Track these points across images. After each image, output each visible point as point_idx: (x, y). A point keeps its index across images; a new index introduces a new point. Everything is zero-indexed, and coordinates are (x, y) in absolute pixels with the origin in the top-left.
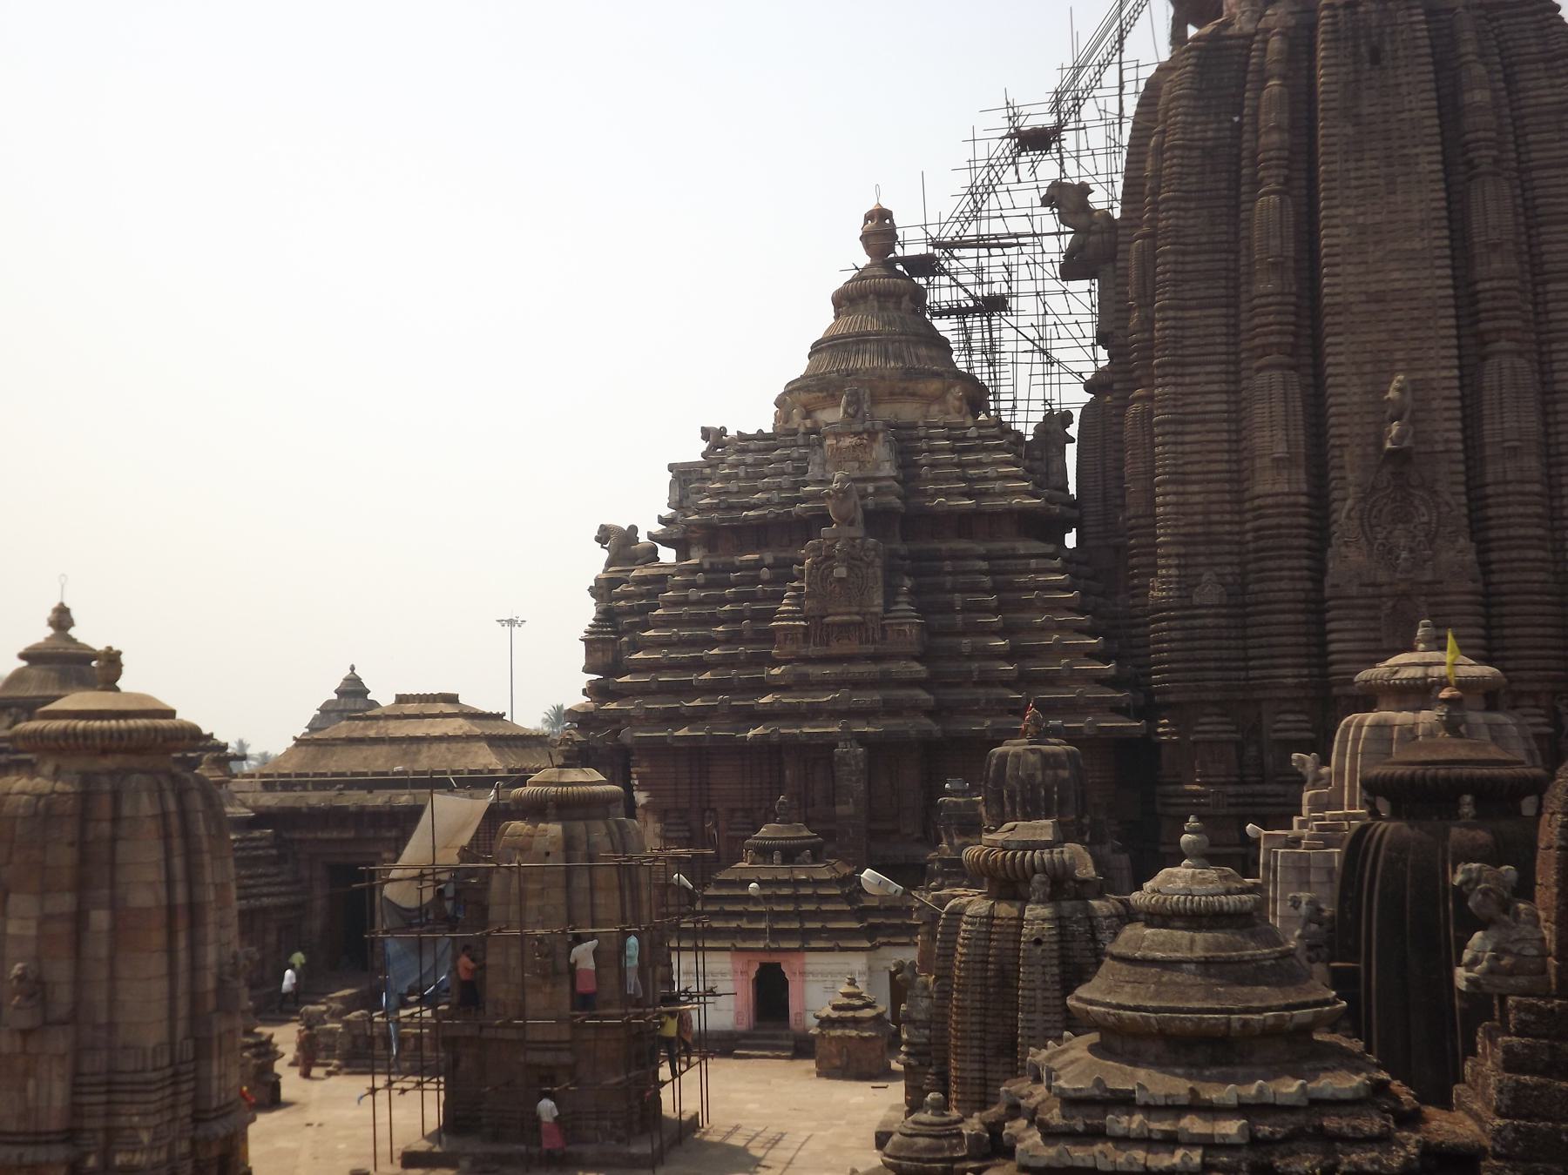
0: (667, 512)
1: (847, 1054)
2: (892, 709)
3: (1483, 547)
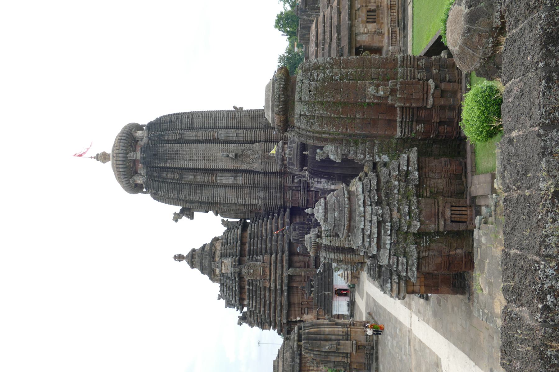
0: (236, 309)
1: (355, 278)
3: (256, 141)
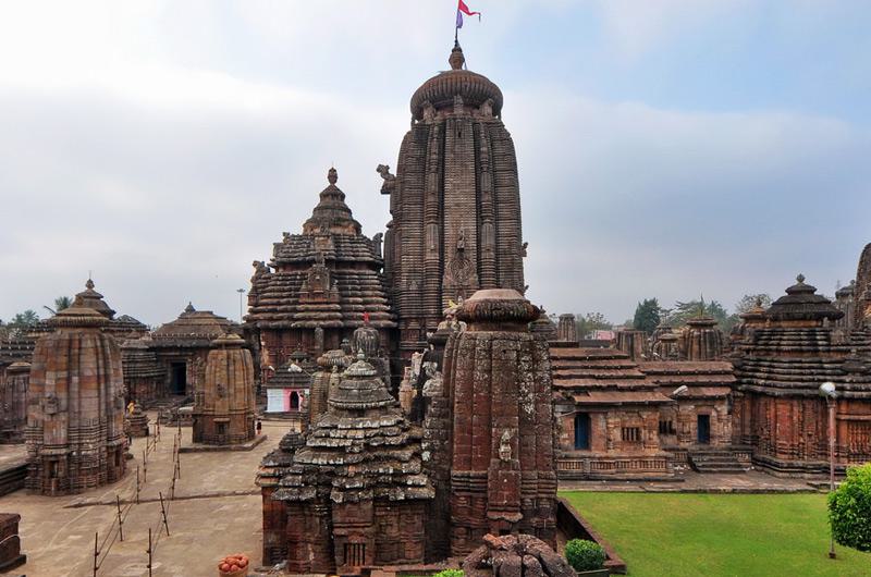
2: (330, 318)
